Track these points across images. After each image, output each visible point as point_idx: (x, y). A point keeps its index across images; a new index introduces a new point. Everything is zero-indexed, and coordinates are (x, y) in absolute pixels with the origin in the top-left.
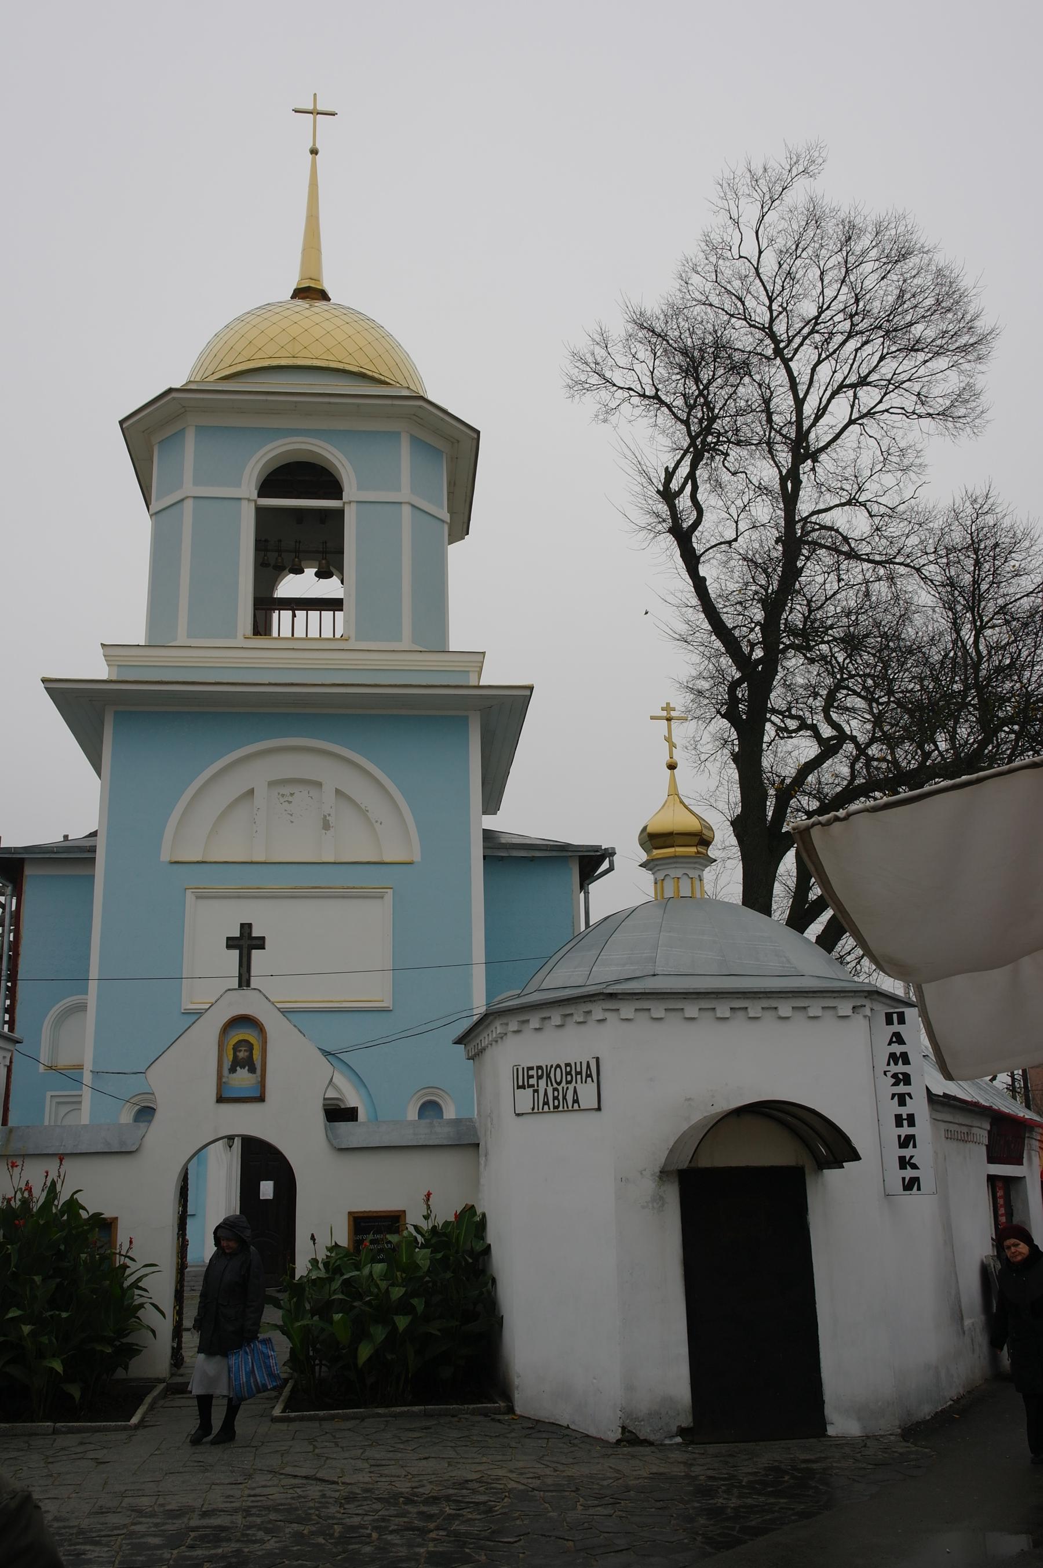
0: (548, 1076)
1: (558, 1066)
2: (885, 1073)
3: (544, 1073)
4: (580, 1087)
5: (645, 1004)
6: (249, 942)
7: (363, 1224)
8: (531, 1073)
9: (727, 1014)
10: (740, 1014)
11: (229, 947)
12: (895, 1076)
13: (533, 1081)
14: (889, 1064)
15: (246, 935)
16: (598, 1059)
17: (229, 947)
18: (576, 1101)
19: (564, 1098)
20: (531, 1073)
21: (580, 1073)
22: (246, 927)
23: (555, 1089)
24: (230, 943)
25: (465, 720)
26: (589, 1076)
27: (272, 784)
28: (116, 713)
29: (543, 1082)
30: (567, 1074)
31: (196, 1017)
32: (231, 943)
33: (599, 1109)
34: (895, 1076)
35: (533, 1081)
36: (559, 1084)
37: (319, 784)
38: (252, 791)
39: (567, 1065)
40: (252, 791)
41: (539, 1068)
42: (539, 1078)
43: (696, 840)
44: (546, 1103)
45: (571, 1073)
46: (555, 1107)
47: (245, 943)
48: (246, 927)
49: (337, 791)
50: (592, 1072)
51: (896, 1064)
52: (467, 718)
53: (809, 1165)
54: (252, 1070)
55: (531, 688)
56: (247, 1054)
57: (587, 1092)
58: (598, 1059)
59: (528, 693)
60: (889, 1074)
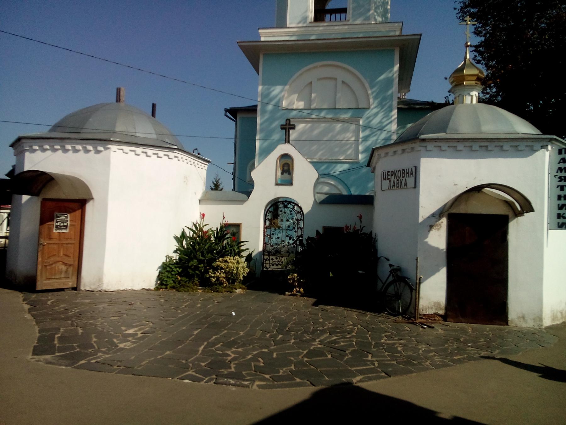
0: (395, 174)
1: (399, 171)
2: (555, 176)
3: (393, 173)
4: (408, 179)
5: (439, 144)
8: (389, 173)
9: (478, 148)
10: (483, 148)
11: (282, 129)
12: (560, 178)
13: (389, 177)
14: (557, 172)
16: (416, 167)
17: (282, 129)
18: (406, 184)
19: (401, 182)
20: (389, 173)
21: (408, 173)
22: (288, 120)
23: (398, 180)
26: (412, 174)
27: (319, 79)
28: (264, 54)
29: (393, 177)
30: (403, 173)
32: (283, 127)
33: (415, 187)
34: (560, 178)
35: (389, 177)
36: (399, 178)
37: (335, 79)
38: (311, 83)
39: (404, 170)
40: (311, 83)
41: (392, 171)
42: (392, 175)
43: (475, 78)
44: (394, 185)
45: (404, 173)
46: (397, 187)
47: (287, 127)
49: (343, 82)
50: (415, 172)
51: (561, 172)
53: (511, 214)
57: (410, 181)
58: (416, 167)
59: (419, 37)
60: (557, 177)
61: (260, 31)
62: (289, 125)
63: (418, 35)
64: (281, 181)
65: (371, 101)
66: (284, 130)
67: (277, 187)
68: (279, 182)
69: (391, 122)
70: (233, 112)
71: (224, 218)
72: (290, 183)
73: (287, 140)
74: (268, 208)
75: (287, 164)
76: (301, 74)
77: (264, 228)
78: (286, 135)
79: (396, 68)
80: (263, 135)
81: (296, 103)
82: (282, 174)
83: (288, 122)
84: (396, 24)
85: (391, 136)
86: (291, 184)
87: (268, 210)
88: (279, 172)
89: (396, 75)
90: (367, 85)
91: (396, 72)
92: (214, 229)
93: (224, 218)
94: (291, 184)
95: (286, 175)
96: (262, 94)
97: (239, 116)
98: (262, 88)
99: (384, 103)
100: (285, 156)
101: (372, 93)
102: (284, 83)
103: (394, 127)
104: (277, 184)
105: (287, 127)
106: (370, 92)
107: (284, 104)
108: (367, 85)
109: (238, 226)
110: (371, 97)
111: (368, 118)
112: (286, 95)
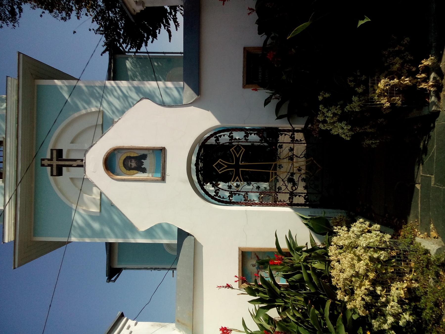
6: (55, 159)
7: (252, 79)
15: (49, 162)
24: (55, 173)
25: (38, 86)
31: (103, 194)
38: (72, 179)
40: (72, 179)
47: (55, 163)
48: (43, 162)
49: (72, 142)
52: (38, 85)
54: (144, 157)
55: (19, 53)
56: (133, 161)
59: (21, 55)
61: (6, 241)
62: (51, 159)
63: (19, 55)
64: (156, 172)
65: (93, 109)
66: (64, 169)
67: (167, 178)
68: (159, 175)
69: (119, 87)
70: (113, 273)
71: (228, 286)
72: (161, 152)
73: (79, 163)
74: (210, 199)
75: (125, 161)
76: (60, 190)
77: (246, 205)
78: (71, 166)
79: (58, 82)
80: (129, 235)
81: (94, 196)
82: (144, 170)
83: (43, 162)
84: (9, 83)
85: (134, 87)
86: (162, 151)
87: (212, 198)
88: (140, 175)
89: (66, 82)
90: (76, 115)
91: (63, 83)
92: (252, 307)
93: (228, 286)
94: (162, 151)
95: (146, 163)
96: (81, 237)
97: (117, 265)
98: (75, 237)
99: (97, 95)
100: (109, 164)
101: (85, 108)
102: (68, 211)
103: (124, 84)
104: (163, 179)
105: (55, 163)
106: (84, 112)
107: (95, 209)
108: (76, 115)
109: (244, 255)
110: (89, 110)
111: (113, 112)
112: (84, 208)
